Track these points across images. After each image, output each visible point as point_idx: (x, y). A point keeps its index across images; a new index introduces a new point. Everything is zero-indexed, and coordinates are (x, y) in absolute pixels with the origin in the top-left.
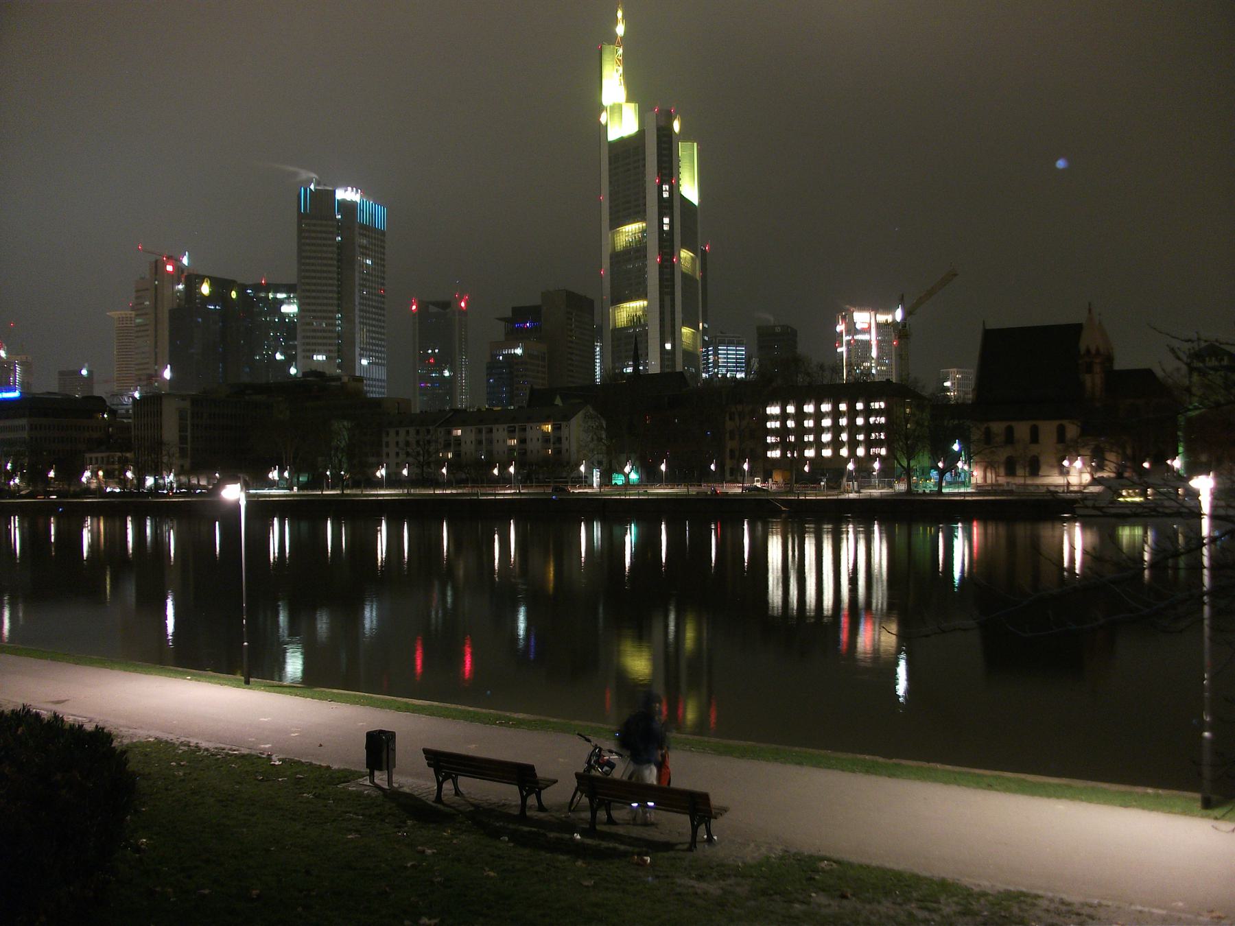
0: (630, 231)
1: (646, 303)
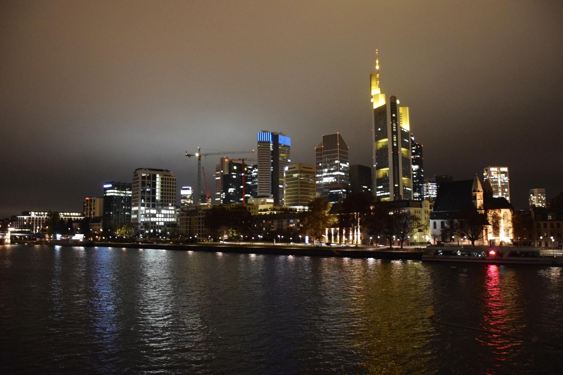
0: (383, 141)
1: (388, 169)
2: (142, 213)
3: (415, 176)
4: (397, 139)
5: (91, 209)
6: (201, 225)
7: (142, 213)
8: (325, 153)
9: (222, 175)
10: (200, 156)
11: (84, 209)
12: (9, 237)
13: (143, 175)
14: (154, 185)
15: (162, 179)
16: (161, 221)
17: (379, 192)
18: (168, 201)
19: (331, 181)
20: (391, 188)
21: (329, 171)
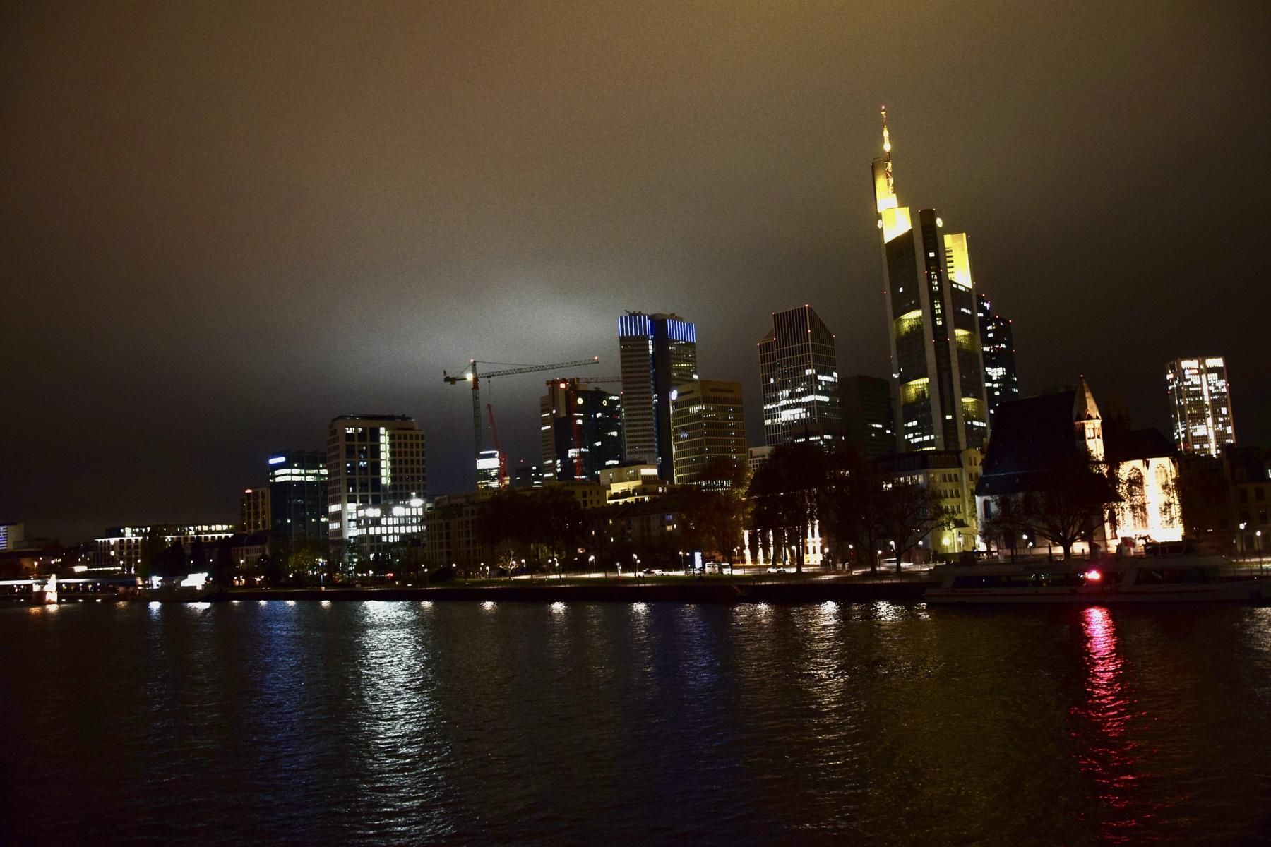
0: (911, 317)
1: (927, 380)
2: (351, 518)
3: (997, 393)
4: (942, 308)
5: (257, 514)
6: (471, 539)
7: (351, 518)
8: (780, 354)
9: (555, 421)
10: (476, 380)
11: (243, 514)
12: (54, 588)
13: (350, 431)
14: (376, 452)
15: (392, 437)
16: (394, 534)
17: (911, 436)
18: (407, 488)
19: (797, 417)
20: (937, 423)
21: (792, 396)
